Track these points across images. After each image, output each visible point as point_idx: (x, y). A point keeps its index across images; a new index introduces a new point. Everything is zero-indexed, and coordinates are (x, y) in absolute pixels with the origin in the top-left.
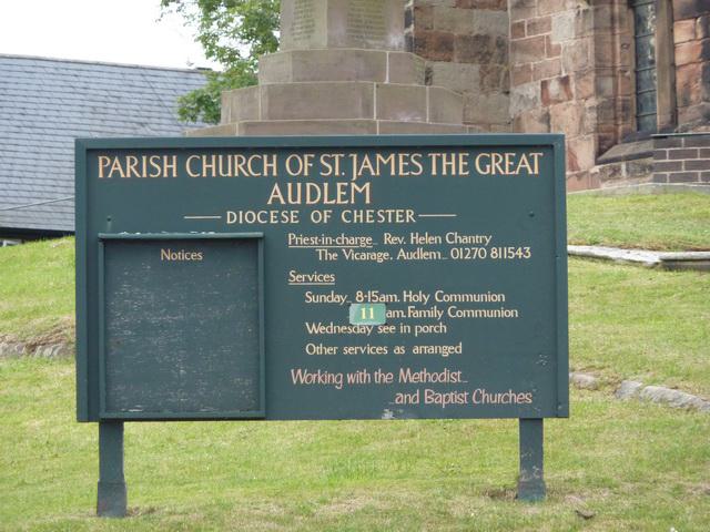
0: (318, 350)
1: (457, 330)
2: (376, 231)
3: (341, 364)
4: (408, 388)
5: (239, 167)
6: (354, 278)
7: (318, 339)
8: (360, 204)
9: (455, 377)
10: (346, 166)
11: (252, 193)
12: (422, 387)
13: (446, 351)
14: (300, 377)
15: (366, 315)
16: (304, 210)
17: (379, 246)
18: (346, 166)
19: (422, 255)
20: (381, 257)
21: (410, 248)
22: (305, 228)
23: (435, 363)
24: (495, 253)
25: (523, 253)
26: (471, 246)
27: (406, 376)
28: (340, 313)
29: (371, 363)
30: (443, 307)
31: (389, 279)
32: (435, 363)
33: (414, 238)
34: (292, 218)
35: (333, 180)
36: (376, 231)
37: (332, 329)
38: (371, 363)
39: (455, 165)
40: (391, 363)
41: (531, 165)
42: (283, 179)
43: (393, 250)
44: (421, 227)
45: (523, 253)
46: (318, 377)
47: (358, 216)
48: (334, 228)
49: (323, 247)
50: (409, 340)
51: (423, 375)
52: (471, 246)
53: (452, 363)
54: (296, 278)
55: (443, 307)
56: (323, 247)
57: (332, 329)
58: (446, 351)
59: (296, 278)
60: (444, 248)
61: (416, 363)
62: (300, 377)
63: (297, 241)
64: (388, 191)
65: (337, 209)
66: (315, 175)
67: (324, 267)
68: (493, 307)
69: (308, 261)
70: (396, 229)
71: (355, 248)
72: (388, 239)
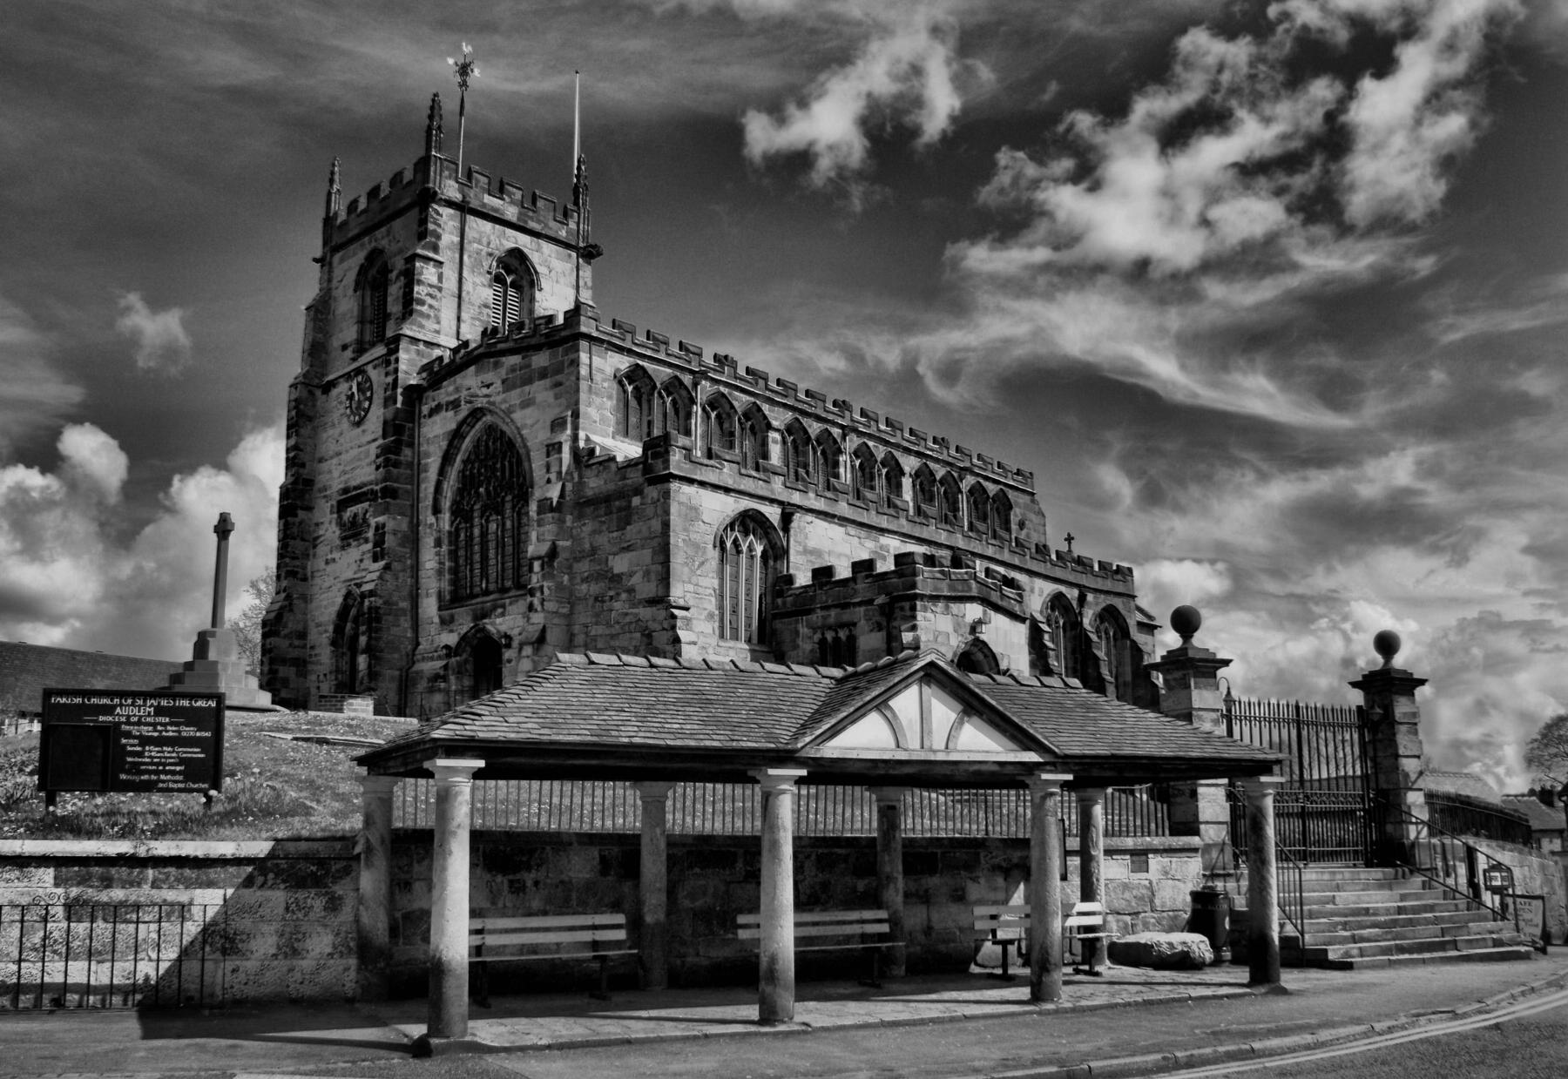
1: (182, 761)
2: (154, 725)
4: (164, 782)
5: (105, 701)
8: (149, 715)
9: (181, 778)
11: (109, 710)
12: (168, 781)
13: (178, 768)
16: (128, 717)
17: (155, 731)
18: (145, 701)
19: (171, 734)
20: (156, 734)
21: (167, 731)
22: (128, 723)
23: (173, 773)
24: (198, 734)
25: (208, 734)
26: (189, 731)
27: (163, 777)
32: (173, 773)
33: (169, 728)
34: (123, 719)
35: (140, 706)
36: (154, 725)
39: (185, 703)
40: (157, 772)
41: (213, 704)
42: (121, 705)
43: (161, 732)
44: (171, 724)
45: (208, 734)
47: (148, 719)
48: (139, 723)
50: (165, 765)
51: (169, 777)
52: (189, 731)
53: (180, 773)
54: (124, 741)
56: (135, 730)
58: (178, 768)
59: (124, 741)
61: (166, 773)
63: (125, 728)
64: (159, 711)
65: (141, 717)
66: (133, 704)
67: (135, 737)
68: (196, 753)
69: (128, 735)
70: (161, 724)
71: (146, 731)
72: (159, 728)
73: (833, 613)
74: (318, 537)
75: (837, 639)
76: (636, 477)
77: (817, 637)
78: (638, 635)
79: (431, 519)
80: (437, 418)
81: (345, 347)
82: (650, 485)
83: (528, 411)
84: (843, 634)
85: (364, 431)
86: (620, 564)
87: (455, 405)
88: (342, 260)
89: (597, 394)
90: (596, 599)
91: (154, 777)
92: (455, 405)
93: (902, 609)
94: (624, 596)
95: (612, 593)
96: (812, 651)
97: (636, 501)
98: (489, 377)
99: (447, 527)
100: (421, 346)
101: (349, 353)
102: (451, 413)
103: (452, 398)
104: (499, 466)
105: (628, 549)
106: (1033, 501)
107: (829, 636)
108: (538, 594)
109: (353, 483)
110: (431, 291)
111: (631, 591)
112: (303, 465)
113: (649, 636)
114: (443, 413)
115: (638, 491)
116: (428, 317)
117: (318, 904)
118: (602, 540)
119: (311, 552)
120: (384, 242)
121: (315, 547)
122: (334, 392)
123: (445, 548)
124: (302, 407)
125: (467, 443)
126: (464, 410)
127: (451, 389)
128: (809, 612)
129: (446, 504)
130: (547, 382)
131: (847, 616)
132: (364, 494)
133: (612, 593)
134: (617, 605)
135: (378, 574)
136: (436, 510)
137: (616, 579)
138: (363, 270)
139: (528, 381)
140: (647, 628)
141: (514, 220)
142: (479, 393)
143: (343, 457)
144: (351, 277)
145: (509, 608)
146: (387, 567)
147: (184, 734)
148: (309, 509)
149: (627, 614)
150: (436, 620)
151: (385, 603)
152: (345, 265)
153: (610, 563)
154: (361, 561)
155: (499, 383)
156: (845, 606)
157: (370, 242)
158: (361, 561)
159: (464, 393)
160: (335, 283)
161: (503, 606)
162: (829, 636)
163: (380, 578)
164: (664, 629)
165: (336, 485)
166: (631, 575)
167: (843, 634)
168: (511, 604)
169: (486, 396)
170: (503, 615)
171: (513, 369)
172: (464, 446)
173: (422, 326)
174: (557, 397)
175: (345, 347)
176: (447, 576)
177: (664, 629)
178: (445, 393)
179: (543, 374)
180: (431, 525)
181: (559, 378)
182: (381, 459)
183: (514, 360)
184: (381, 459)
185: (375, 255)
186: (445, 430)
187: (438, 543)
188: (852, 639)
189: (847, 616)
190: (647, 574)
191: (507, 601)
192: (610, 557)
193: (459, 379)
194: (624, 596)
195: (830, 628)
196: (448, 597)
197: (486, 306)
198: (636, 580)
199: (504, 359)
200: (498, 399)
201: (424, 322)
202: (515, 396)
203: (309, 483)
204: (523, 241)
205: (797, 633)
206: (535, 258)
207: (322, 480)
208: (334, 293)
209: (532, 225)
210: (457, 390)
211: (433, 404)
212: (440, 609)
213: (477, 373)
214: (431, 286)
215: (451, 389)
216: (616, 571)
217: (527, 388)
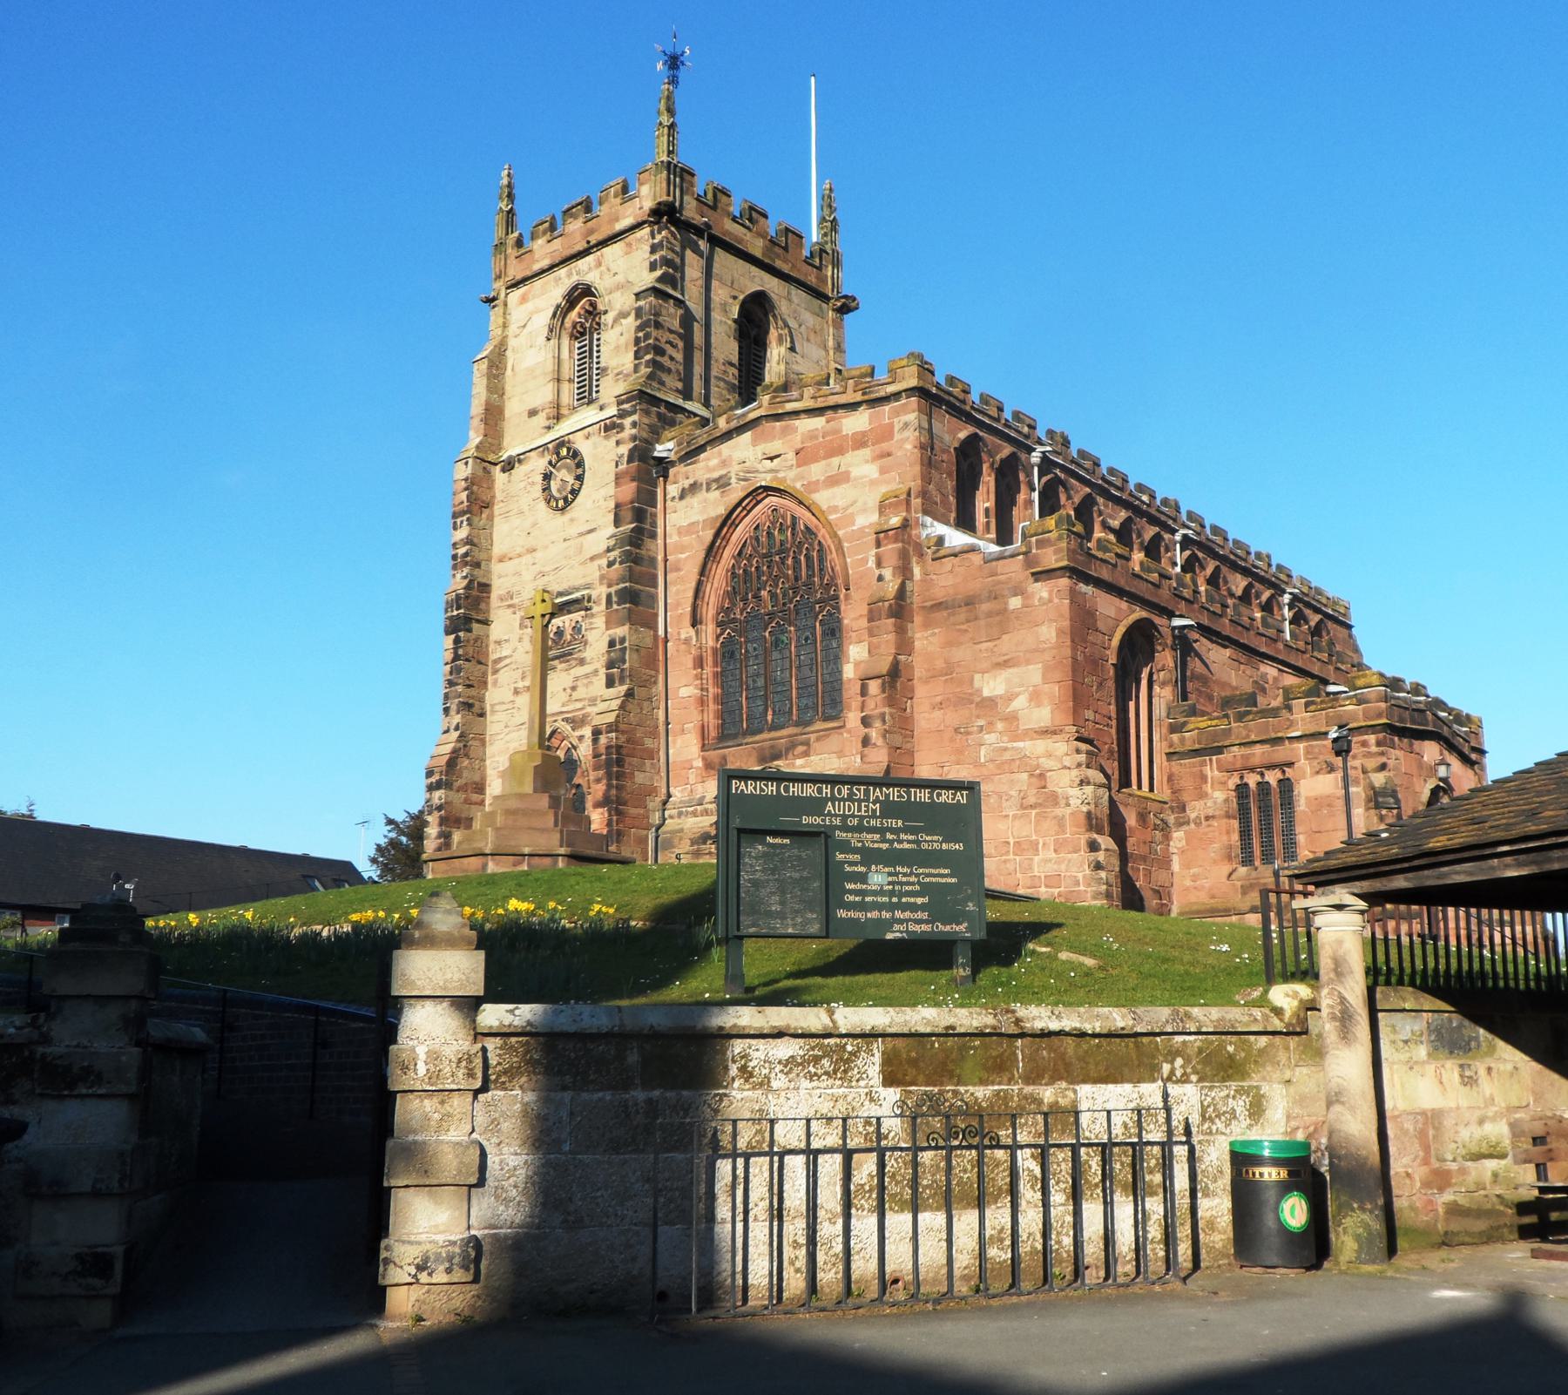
0: (851, 898)
1: (926, 889)
2: (881, 831)
3: (862, 906)
4: (901, 922)
5: (809, 790)
6: (871, 857)
7: (851, 892)
8: (874, 816)
9: (924, 916)
10: (867, 792)
11: (816, 806)
12: (907, 921)
13: (919, 901)
14: (842, 914)
15: (878, 878)
16: (844, 817)
17: (884, 840)
18: (867, 792)
19: (906, 846)
20: (885, 846)
21: (900, 842)
22: (845, 828)
23: (913, 908)
24: (945, 846)
25: (958, 847)
26: (932, 842)
27: (898, 914)
28: (862, 878)
29: (880, 907)
30: (917, 875)
31: (891, 858)
32: (913, 908)
33: (902, 836)
34: (837, 822)
35: (860, 801)
36: (881, 831)
37: (859, 886)
38: (880, 907)
39: (923, 796)
40: (891, 907)
41: (962, 797)
42: (833, 799)
43: (891, 842)
44: (906, 830)
45: (958, 847)
46: (851, 914)
47: (873, 822)
48: (859, 829)
49: (854, 839)
50: (901, 894)
51: (907, 914)
52: (932, 842)
53: (923, 907)
54: (840, 857)
55: (917, 875)
56: (854, 839)
57: (859, 886)
58: (919, 901)
59: (840, 857)
60: (917, 842)
62: (842, 914)
63: (840, 835)
64: (889, 809)
65: (862, 818)
66: (851, 798)
67: (855, 851)
68: (943, 876)
69: (845, 847)
72: (889, 836)
73: (1258, 750)
74: (500, 659)
75: (1263, 787)
76: (1014, 569)
77: (1234, 781)
78: (1025, 776)
79: (688, 632)
80: (695, 501)
81: (533, 413)
82: (1036, 581)
83: (838, 490)
84: (1272, 778)
85: (572, 520)
86: (992, 685)
87: (722, 483)
88: (524, 299)
89: (937, 469)
90: (956, 730)
91: (886, 915)
92: (722, 483)
93: (1364, 744)
94: (1000, 726)
95: (981, 722)
96: (1227, 800)
97: (1015, 603)
98: (774, 447)
99: (711, 643)
100: (663, 410)
101: (541, 420)
102: (715, 494)
103: (716, 475)
104: (790, 561)
105: (1005, 664)
106: (1350, 636)
107: (1252, 780)
108: (878, 724)
109: (555, 588)
110: (672, 337)
111: (1012, 718)
112: (477, 565)
113: (1042, 776)
114: (702, 495)
115: (1018, 591)
116: (669, 371)
117: (1240, 1105)
118: (961, 654)
119: (490, 679)
120: (592, 278)
121: (496, 672)
122: (519, 470)
123: (709, 670)
124: (475, 488)
125: (741, 532)
126: (737, 492)
127: (714, 462)
128: (1219, 750)
129: (709, 611)
130: (866, 452)
131: (1281, 753)
132: (576, 601)
133: (981, 722)
134: (990, 738)
135: (619, 702)
136: (695, 621)
137: (989, 704)
138: (561, 312)
139: (840, 451)
140: (1038, 766)
141: (758, 253)
142: (760, 467)
143: (538, 555)
144: (543, 319)
145: (815, 745)
146: (629, 694)
147: (925, 846)
148: (486, 622)
149: (1006, 749)
150: (699, 763)
151: (628, 741)
152: (530, 306)
153: (977, 684)
154: (574, 688)
155: (791, 455)
156: (1277, 741)
157: (569, 275)
158: (574, 688)
159: (734, 470)
160: (513, 329)
161: (807, 743)
162: (1252, 780)
163: (622, 707)
164: (1065, 767)
165: (527, 591)
166: (1010, 698)
167: (1272, 778)
168: (818, 739)
169: (772, 471)
170: (806, 754)
171: (812, 435)
172: (734, 538)
173: (662, 383)
174: (883, 471)
175: (533, 413)
176: (712, 707)
177: (1065, 767)
178: (708, 464)
179: (860, 441)
180: (687, 641)
181: (885, 446)
182: (616, 553)
183: (818, 422)
184: (616, 553)
185: (581, 293)
186: (705, 517)
187: (699, 663)
188: (1286, 786)
189: (1281, 753)
190: (1035, 697)
191: (813, 737)
192: (977, 677)
193: (726, 448)
194: (1000, 726)
195: (1252, 770)
196: (713, 734)
197: (731, 364)
198: (1020, 703)
199: (797, 423)
200: (791, 474)
201: (665, 377)
202: (817, 471)
203: (485, 587)
204: (772, 285)
205: (1204, 778)
206: (783, 307)
207: (499, 587)
208: (512, 342)
209: (779, 264)
210: (724, 463)
211: (686, 484)
212: (704, 748)
213: (755, 443)
214: (671, 331)
215: (714, 462)
216: (986, 693)
217: (835, 461)
